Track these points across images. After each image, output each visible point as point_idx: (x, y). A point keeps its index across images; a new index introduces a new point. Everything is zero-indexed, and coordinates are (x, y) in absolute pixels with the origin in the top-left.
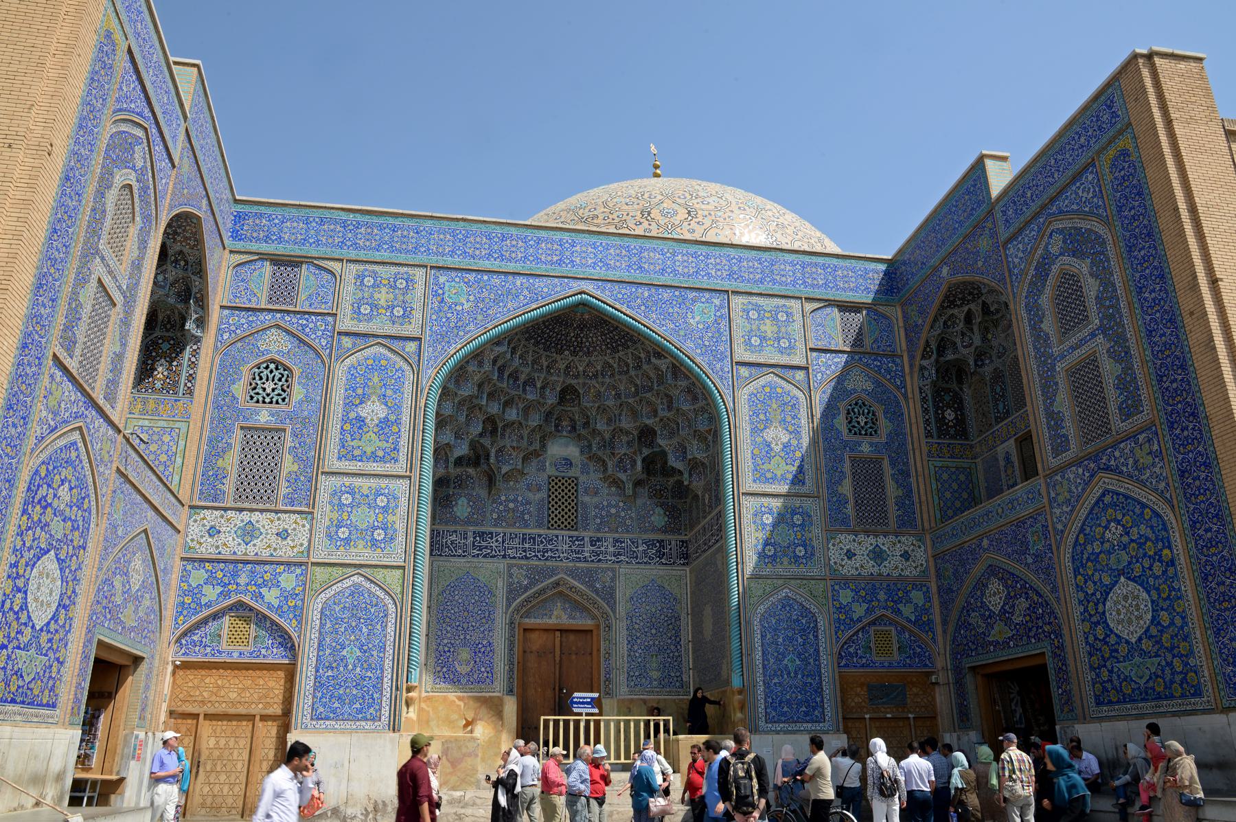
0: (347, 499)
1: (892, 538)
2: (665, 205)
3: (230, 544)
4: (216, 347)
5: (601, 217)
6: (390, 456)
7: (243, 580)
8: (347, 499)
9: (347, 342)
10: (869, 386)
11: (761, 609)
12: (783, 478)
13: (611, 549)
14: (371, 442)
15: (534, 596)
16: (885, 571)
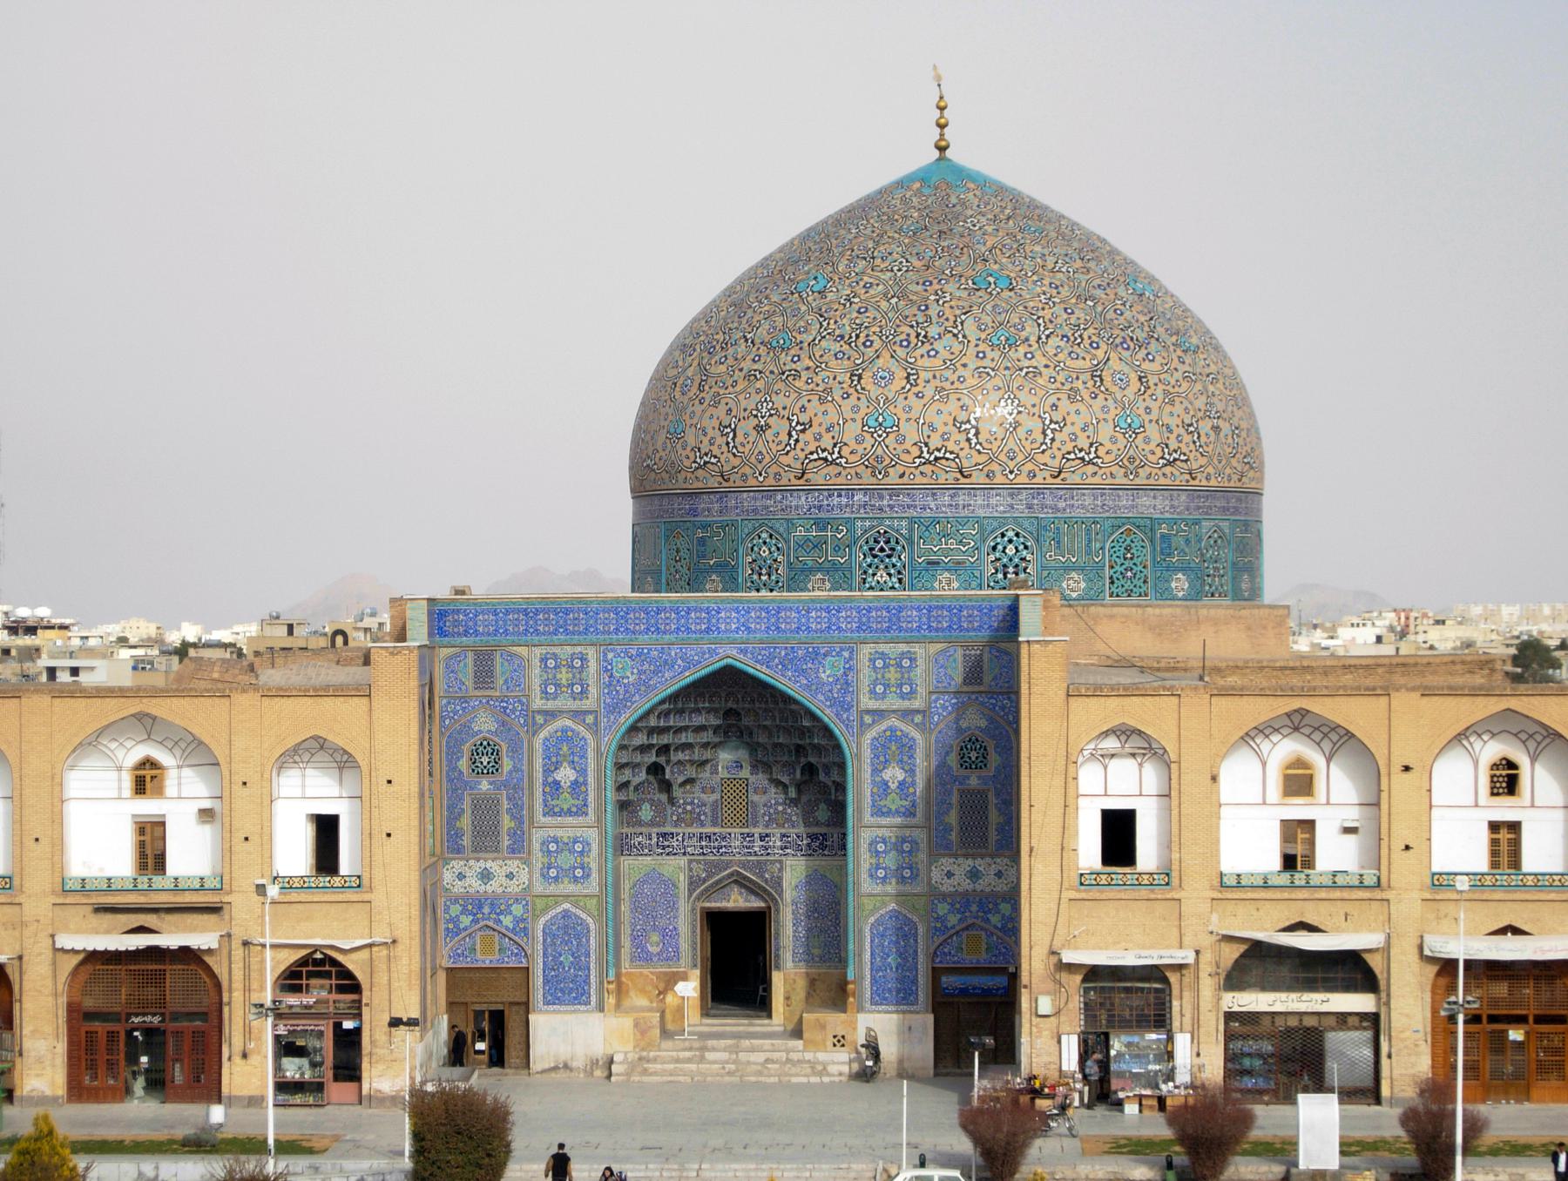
0: (553, 847)
1: (988, 860)
2: (881, 360)
3: (474, 884)
4: (442, 734)
5: (804, 378)
6: (581, 811)
7: (486, 910)
8: (553, 847)
9: (540, 719)
10: (983, 723)
11: (872, 920)
12: (897, 811)
13: (779, 843)
14: (566, 801)
15: (712, 886)
16: (979, 888)
